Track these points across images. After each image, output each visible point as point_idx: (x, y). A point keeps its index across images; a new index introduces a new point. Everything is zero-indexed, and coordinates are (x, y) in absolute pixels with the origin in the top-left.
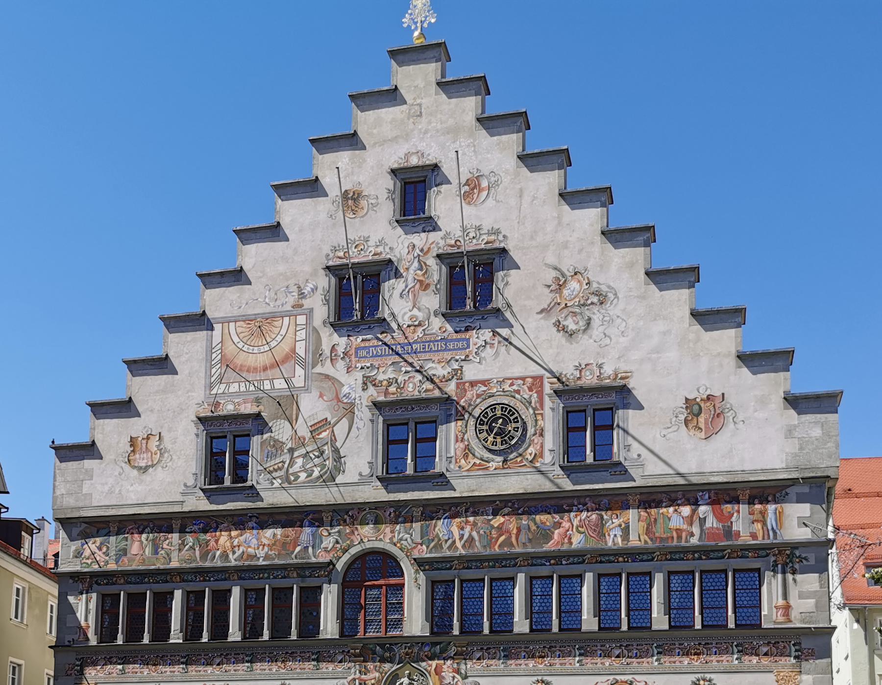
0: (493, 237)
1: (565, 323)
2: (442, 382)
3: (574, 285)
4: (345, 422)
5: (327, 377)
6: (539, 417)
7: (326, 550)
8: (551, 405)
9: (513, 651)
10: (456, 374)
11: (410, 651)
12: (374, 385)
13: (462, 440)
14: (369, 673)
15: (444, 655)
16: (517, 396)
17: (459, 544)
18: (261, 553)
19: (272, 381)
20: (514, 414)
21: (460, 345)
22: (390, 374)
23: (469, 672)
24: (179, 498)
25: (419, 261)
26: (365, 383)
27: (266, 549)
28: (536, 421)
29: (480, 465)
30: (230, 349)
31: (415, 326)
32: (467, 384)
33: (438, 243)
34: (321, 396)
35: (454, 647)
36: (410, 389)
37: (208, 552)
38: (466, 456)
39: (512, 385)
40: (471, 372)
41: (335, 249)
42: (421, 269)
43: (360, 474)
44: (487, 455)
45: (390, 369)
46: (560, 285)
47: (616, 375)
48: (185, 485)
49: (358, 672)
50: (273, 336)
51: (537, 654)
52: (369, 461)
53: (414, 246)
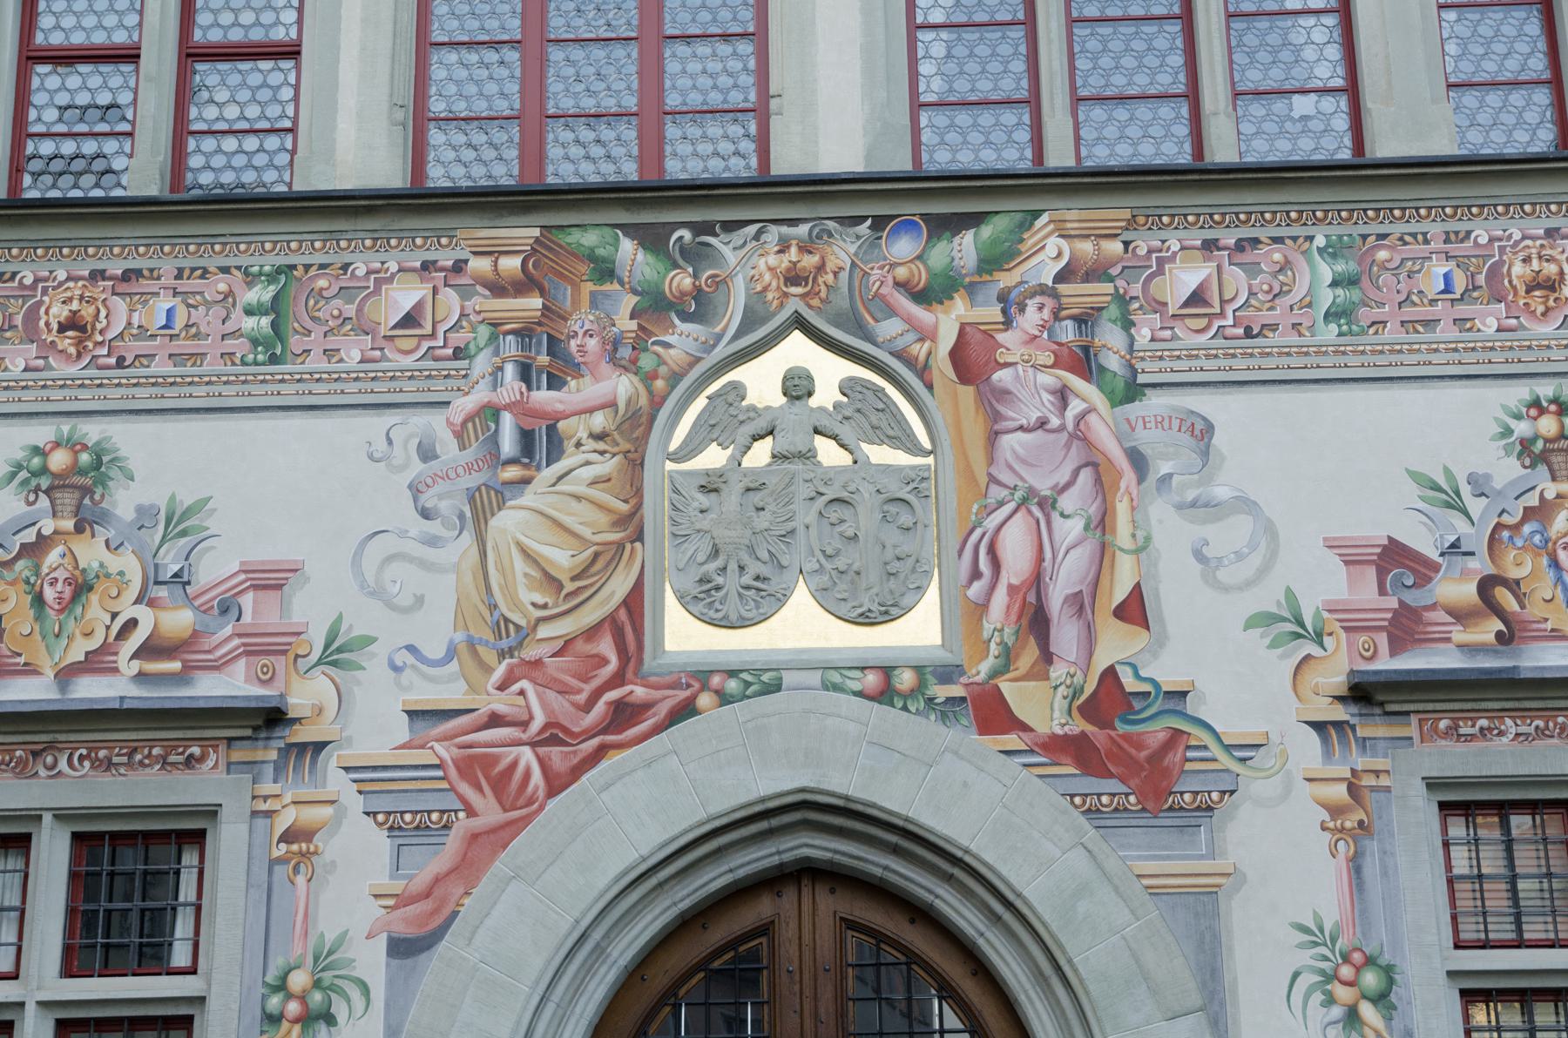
9: (1382, 255)
11: (810, 261)
14: (578, 375)
15: (1005, 280)
23: (1147, 365)
35: (1053, 244)
49: (510, 369)
51: (1518, 269)
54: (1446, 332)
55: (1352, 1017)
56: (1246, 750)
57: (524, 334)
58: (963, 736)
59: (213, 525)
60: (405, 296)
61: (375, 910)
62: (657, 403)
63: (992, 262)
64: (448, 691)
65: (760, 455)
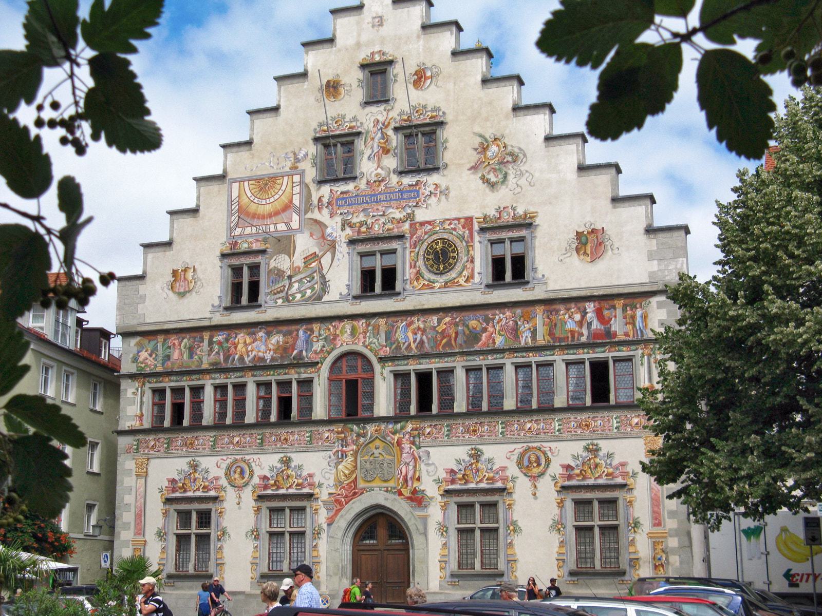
0: (435, 114)
1: (489, 177)
2: (399, 222)
3: (494, 148)
4: (329, 255)
5: (316, 221)
6: (470, 248)
7: (315, 352)
8: (479, 239)
10: (409, 217)
12: (350, 227)
13: (415, 266)
15: (403, 431)
16: (454, 233)
17: (413, 346)
18: (268, 356)
19: (275, 224)
20: (452, 246)
21: (412, 194)
22: (362, 218)
24: (209, 315)
25: (382, 132)
26: (343, 225)
27: (272, 352)
28: (468, 251)
29: (428, 285)
30: (245, 200)
31: (380, 181)
32: (418, 225)
33: (395, 119)
34: (311, 235)
36: (376, 229)
37: (229, 356)
38: (417, 279)
39: (450, 224)
40: (421, 215)
41: (321, 125)
42: (383, 138)
43: (341, 294)
44: (433, 277)
45: (362, 214)
46: (484, 148)
47: (526, 215)
48: (213, 306)
50: (276, 191)
52: (347, 283)
53: (378, 121)
54: (461, 438)
55: (442, 534)
56: (431, 498)
57: (342, 440)
58: (397, 497)
59: (304, 468)
60: (327, 434)
61: (325, 520)
62: (359, 449)
63: (402, 428)
64: (333, 490)
65: (372, 458)
